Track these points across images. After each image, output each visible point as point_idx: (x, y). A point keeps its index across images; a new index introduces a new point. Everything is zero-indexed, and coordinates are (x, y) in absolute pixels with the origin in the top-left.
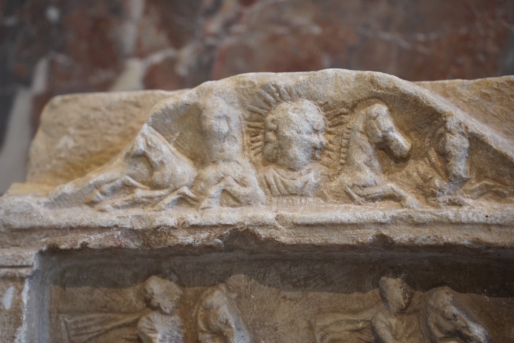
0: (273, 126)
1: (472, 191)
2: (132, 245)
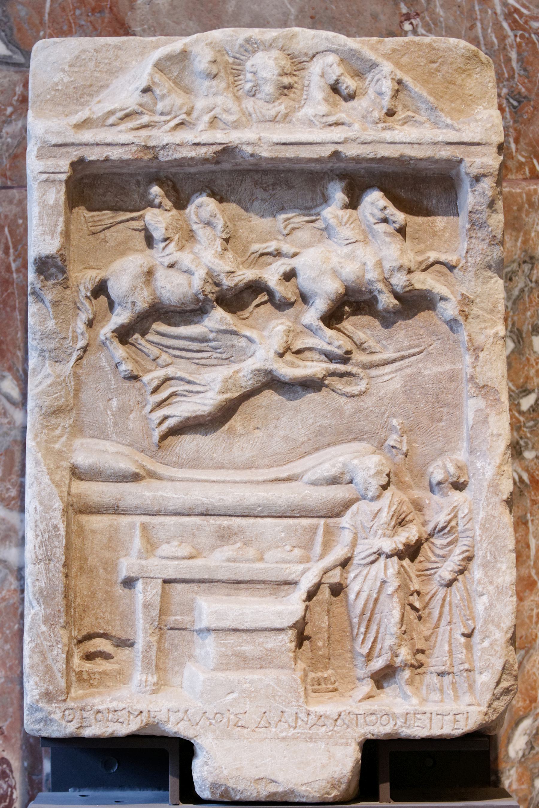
0: (253, 69)
1: (400, 120)
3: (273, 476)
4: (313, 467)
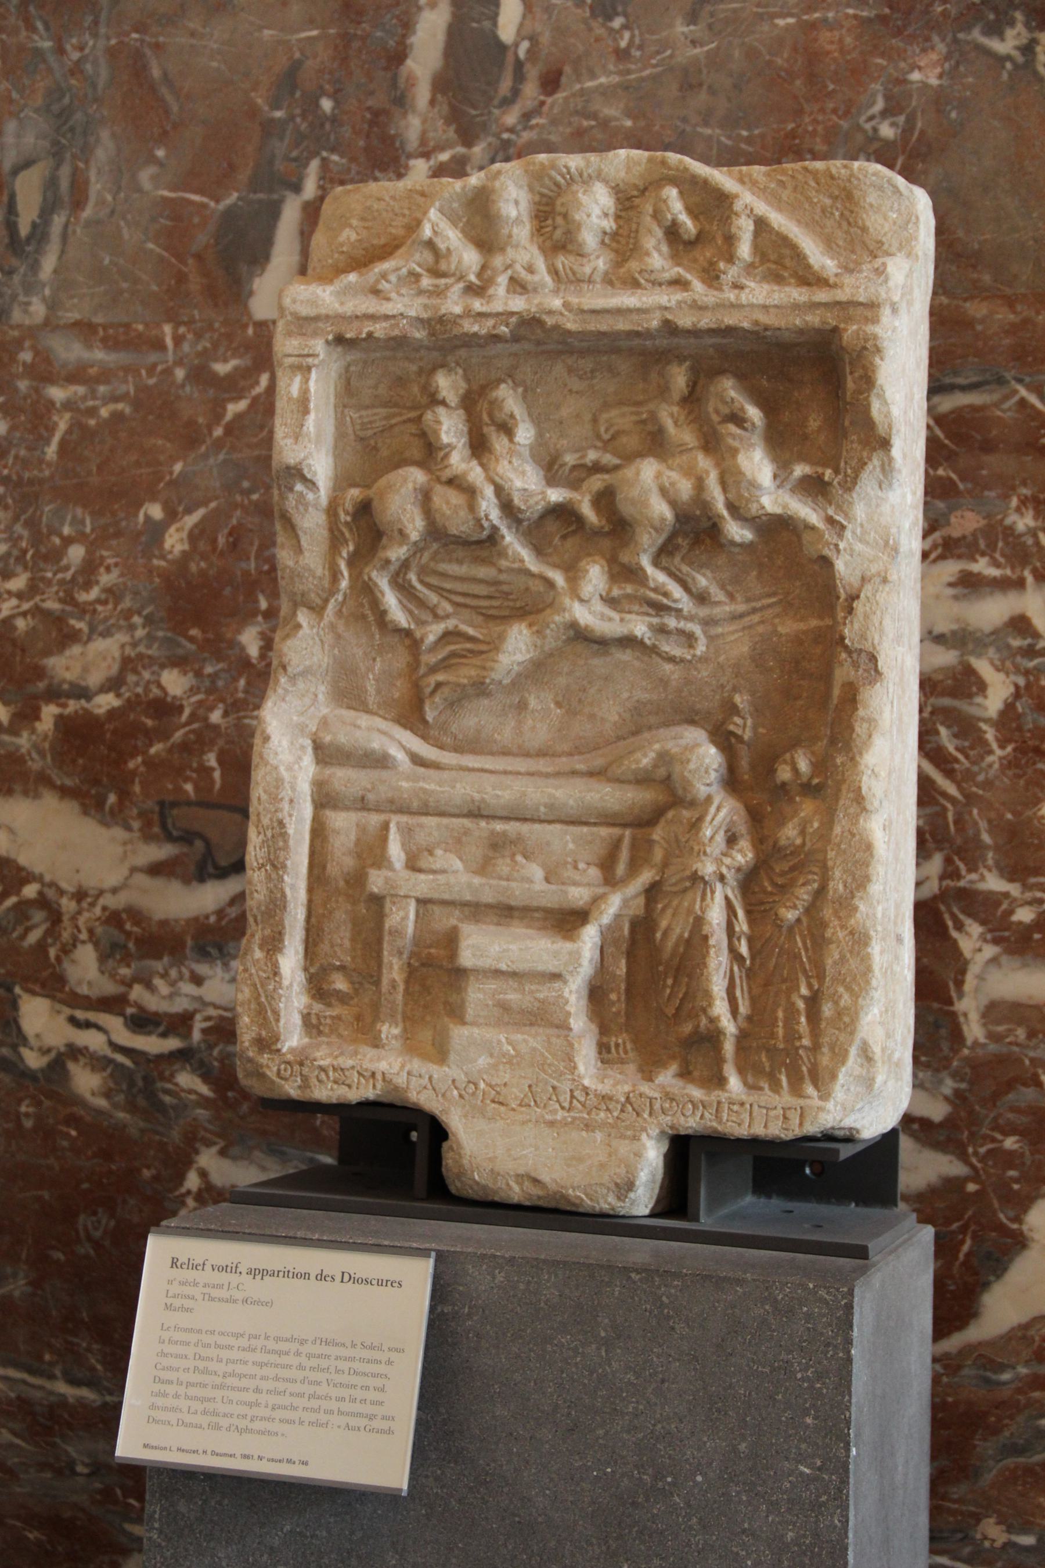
0: (563, 210)
2: (418, 335)
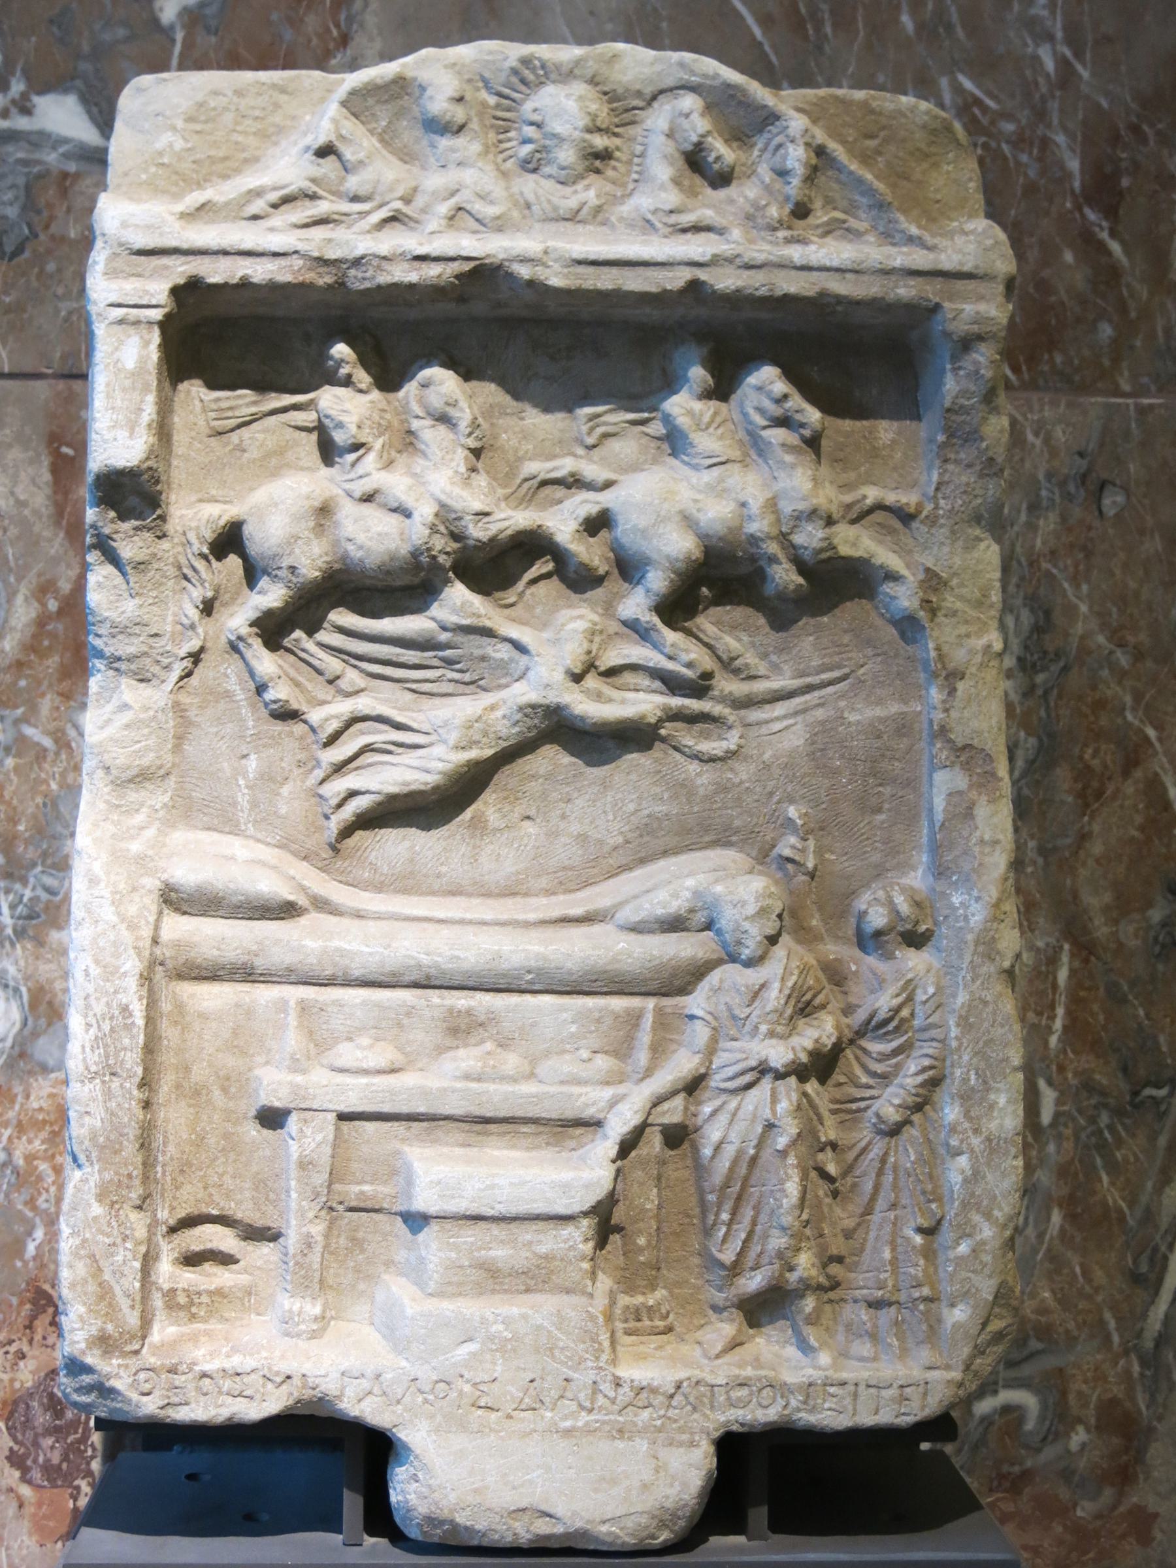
0: (536, 117)
1: (818, 227)
2: (321, 282)
3: (556, 913)
4: (636, 897)
